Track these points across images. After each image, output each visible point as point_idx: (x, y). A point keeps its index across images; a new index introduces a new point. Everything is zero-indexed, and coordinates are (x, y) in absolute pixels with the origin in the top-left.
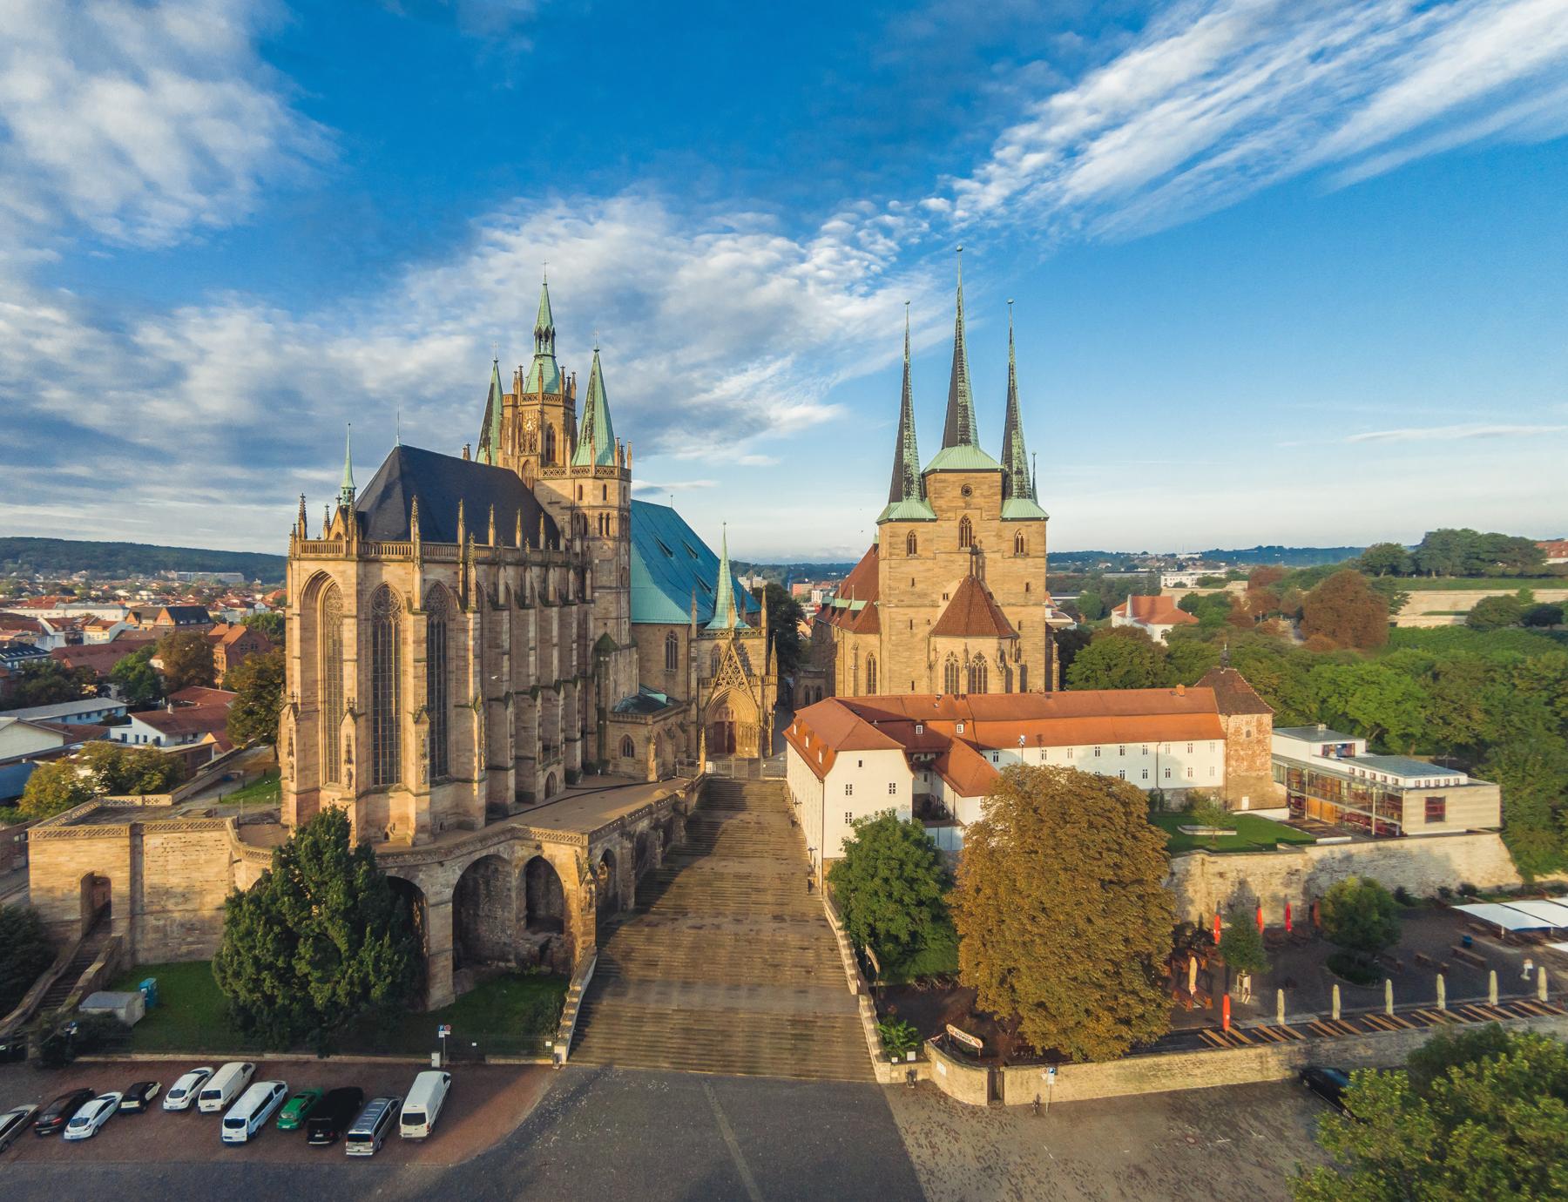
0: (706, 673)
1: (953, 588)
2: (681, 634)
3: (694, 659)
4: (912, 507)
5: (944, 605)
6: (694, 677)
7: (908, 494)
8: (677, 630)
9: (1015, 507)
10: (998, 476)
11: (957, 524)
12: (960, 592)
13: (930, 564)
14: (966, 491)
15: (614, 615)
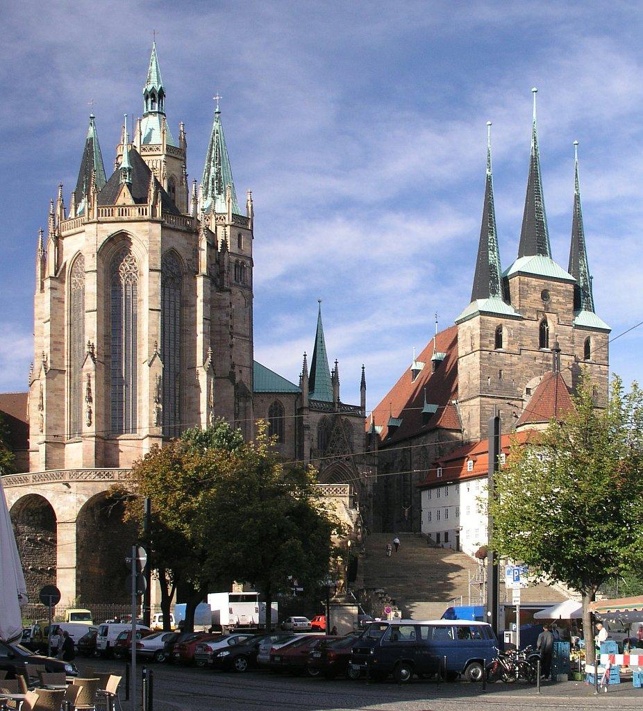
0: (315, 445)
1: (534, 383)
2: (288, 404)
3: (308, 428)
4: (495, 304)
5: (528, 399)
6: (307, 444)
7: (494, 292)
8: (283, 400)
9: (584, 318)
10: (570, 287)
11: (537, 324)
12: (544, 386)
13: (515, 359)
14: (545, 295)
15: (247, 363)
